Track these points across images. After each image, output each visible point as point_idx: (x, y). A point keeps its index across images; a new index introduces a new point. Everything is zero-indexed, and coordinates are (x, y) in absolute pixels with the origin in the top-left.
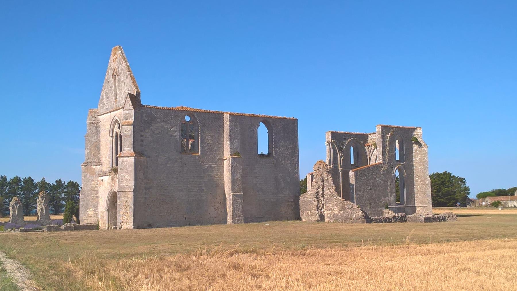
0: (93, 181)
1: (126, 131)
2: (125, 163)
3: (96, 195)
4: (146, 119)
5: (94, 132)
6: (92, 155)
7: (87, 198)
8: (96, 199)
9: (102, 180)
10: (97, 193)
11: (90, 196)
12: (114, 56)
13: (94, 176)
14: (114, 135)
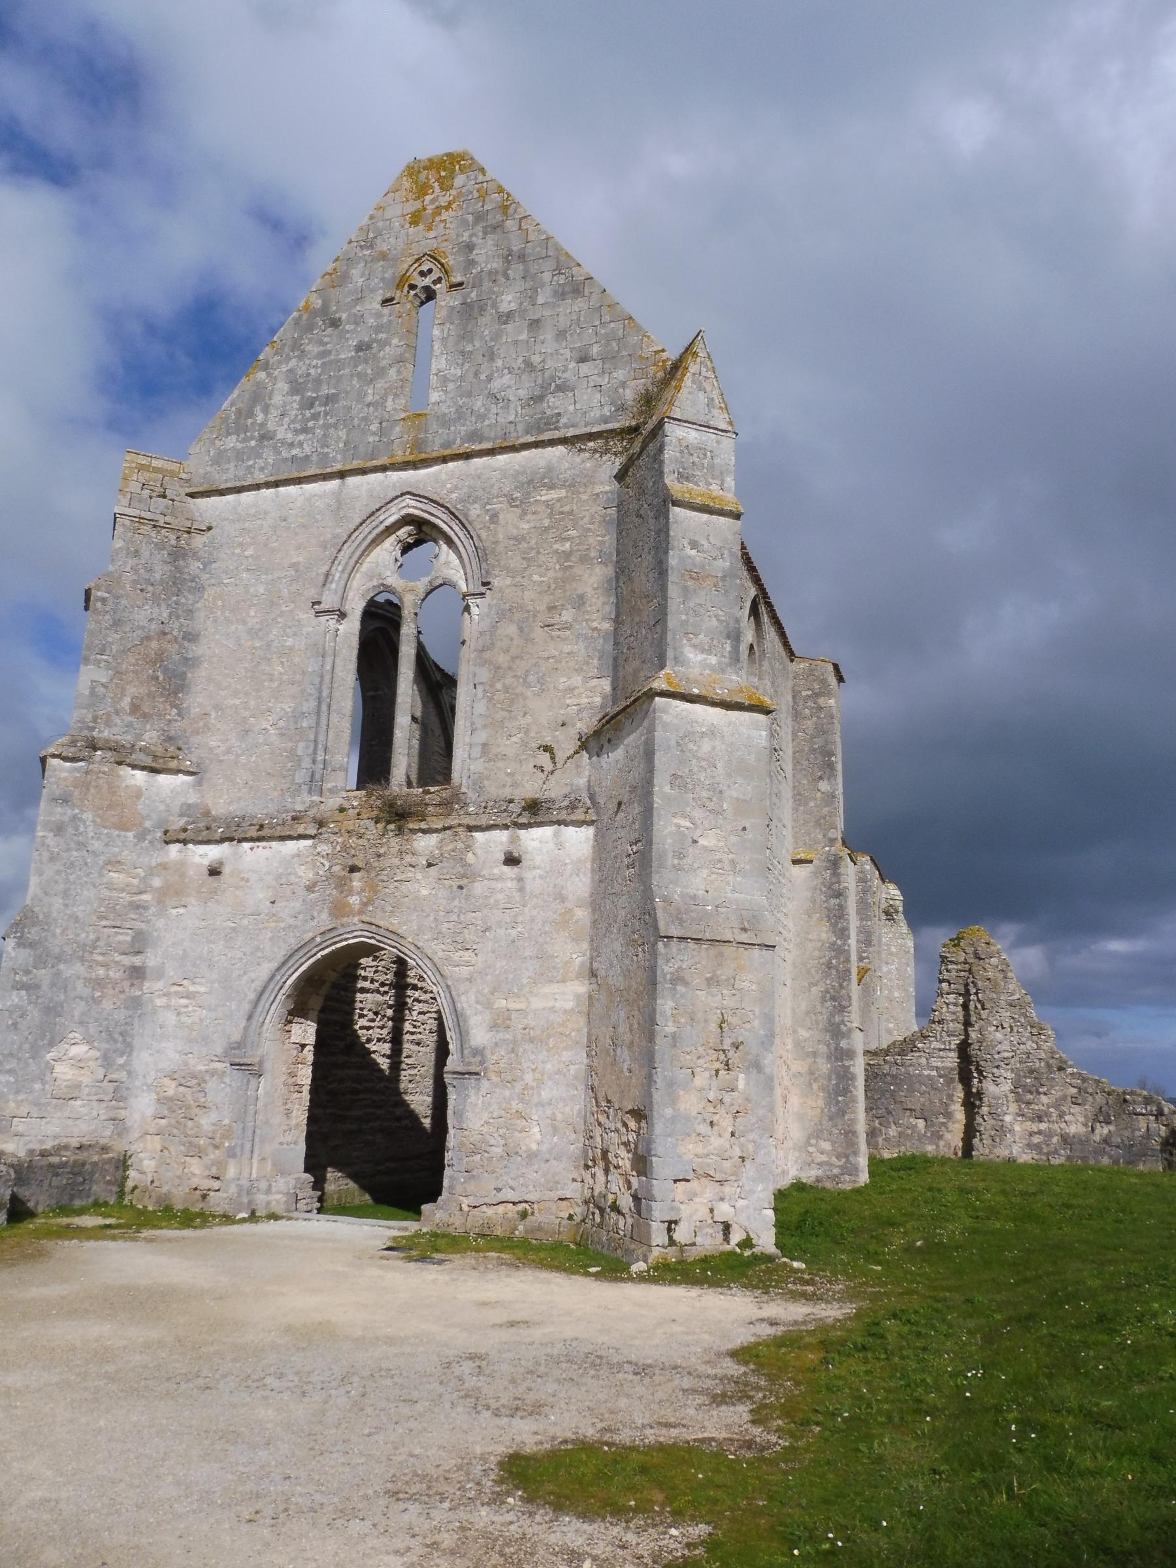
0: (115, 864)
1: (694, 545)
2: (706, 746)
3: (127, 961)
5: (157, 576)
6: (127, 709)
7: (58, 974)
8: (126, 984)
10: (137, 947)
11: (82, 959)
12: (428, 198)
13: (130, 835)
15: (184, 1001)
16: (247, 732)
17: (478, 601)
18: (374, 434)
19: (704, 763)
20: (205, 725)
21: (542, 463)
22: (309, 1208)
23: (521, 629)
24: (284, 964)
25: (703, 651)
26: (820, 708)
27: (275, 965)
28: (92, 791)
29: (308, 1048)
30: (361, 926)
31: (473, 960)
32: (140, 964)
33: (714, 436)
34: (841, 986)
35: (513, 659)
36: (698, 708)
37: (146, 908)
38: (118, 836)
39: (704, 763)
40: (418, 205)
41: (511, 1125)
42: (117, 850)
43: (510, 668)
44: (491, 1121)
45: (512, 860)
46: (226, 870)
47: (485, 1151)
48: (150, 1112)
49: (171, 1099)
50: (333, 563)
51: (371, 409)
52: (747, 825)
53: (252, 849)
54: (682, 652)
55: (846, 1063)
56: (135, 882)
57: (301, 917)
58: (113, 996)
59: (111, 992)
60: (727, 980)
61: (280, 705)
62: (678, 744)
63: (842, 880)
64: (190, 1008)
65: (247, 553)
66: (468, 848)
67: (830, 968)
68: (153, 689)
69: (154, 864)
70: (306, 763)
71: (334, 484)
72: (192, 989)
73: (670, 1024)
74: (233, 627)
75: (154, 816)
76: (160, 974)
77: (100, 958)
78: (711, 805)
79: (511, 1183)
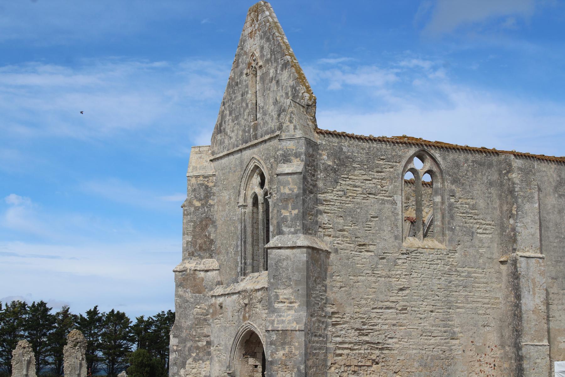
4: (330, 163)
14: (250, 201)
15: (219, 352)
16: (228, 253)
19: (284, 269)
24: (235, 338)
25: (289, 227)
26: (509, 179)
28: (189, 281)
30: (249, 324)
32: (209, 340)
33: (296, 141)
36: (282, 251)
37: (209, 320)
38: (198, 296)
39: (284, 269)
42: (198, 301)
52: (299, 289)
54: (282, 230)
56: (205, 311)
59: (202, 350)
60: (288, 342)
62: (275, 264)
68: (205, 239)
69: (210, 304)
72: (220, 348)
73: (270, 358)
75: (208, 287)
77: (197, 339)
78: (287, 284)
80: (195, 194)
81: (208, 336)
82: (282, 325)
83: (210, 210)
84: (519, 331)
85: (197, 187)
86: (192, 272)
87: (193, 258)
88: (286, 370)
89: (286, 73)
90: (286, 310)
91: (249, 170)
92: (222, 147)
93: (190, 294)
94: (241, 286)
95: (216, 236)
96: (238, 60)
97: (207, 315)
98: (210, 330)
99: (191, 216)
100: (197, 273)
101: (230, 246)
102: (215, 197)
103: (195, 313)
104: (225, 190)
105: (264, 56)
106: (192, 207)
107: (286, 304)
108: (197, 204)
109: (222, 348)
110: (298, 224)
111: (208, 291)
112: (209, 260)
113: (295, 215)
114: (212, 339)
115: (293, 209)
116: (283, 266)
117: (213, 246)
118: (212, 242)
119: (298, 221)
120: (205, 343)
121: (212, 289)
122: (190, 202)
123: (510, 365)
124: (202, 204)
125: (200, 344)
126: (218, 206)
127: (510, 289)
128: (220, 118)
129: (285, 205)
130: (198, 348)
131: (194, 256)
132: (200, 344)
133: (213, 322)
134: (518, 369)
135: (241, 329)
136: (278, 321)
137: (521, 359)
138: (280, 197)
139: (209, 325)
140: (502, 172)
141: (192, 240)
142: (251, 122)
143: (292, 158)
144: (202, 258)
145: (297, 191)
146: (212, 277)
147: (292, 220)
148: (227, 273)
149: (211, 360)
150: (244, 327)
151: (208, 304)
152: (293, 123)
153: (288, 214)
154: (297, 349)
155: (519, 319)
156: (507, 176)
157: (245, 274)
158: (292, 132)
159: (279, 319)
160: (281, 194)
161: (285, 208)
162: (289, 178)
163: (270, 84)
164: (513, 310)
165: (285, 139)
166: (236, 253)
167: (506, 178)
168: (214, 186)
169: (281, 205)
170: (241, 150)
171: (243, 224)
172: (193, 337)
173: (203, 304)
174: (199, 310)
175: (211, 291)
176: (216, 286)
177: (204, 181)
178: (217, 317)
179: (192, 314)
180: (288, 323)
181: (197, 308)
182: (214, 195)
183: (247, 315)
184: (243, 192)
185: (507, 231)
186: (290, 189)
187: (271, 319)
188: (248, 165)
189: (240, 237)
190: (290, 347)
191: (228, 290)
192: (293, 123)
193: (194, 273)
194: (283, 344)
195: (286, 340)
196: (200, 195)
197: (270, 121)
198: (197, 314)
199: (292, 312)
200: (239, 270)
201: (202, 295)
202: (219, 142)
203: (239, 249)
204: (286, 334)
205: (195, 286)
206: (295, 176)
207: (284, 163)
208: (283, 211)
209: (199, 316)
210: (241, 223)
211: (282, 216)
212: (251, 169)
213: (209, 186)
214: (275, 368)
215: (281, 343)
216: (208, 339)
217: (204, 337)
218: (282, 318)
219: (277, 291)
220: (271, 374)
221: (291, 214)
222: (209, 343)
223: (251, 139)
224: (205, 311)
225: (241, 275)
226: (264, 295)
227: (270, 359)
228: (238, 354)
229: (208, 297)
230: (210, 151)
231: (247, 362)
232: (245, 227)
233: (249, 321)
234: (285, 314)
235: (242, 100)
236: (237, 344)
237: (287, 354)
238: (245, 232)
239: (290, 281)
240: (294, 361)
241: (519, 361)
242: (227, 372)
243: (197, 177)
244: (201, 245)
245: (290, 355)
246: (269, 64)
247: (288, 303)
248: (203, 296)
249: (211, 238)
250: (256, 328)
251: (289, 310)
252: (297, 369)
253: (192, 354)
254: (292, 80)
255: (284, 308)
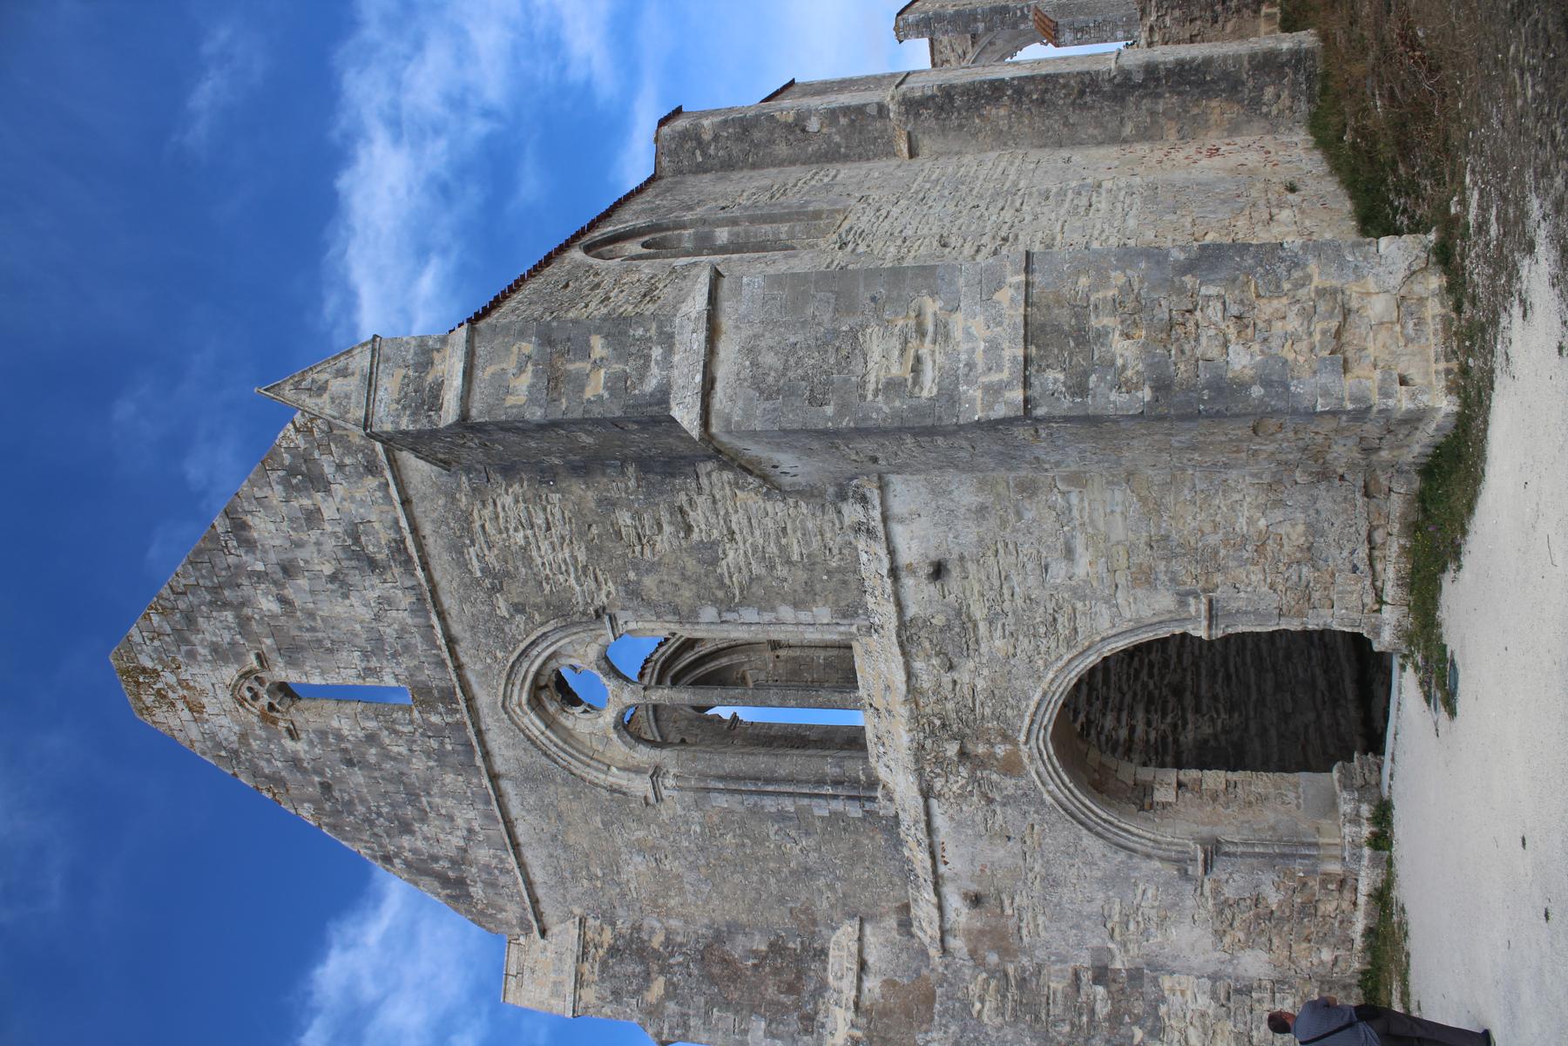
2: (769, 359)
9: (976, 901)
15: (1132, 926)
16: (807, 870)
17: (620, 622)
18: (442, 744)
19: (792, 361)
20: (804, 912)
21: (446, 557)
22: (1375, 768)
23: (648, 571)
24: (1082, 823)
25: (646, 366)
26: (716, 138)
27: (1085, 831)
28: (891, 1035)
29: (1182, 777)
31: (1068, 609)
32: (1090, 973)
34: (1064, 86)
35: (684, 577)
36: (723, 372)
37: (1024, 970)
38: (941, 1004)
39: (792, 361)
40: (180, 705)
41: (1274, 557)
42: (957, 1005)
43: (697, 581)
44: (1269, 580)
45: (938, 571)
46: (974, 888)
47: (1307, 586)
48: (1265, 956)
49: (1249, 934)
50: (596, 785)
51: (415, 747)
53: (946, 863)
54: (651, 395)
55: (1163, 73)
56: (993, 983)
57: (1025, 807)
58: (1129, 1001)
59: (1124, 1004)
60: (1076, 316)
61: (772, 837)
63: (930, 93)
64: (1140, 919)
65: (600, 874)
66: (927, 623)
67: (1043, 102)
68: (767, 969)
69: (971, 963)
70: (838, 806)
71: (506, 785)
72: (1116, 918)
73: (1140, 394)
74: (688, 887)
75: (914, 966)
76: (1101, 953)
77: (1085, 1019)
79: (1345, 554)
80: (628, 991)
81: (1077, 976)
82: (1006, 345)
83: (681, 945)
84: (1082, 82)
85: (607, 984)
86: (863, 1021)
87: (820, 1017)
88: (1191, 326)
89: (257, 521)
90: (950, 349)
91: (548, 738)
92: (502, 880)
93: (934, 1035)
94: (901, 784)
95: (761, 931)
96: (267, 777)
97: (1006, 975)
98: (1058, 967)
99: (691, 1012)
100: (866, 1002)
101: (783, 857)
102: (645, 926)
103: (999, 1020)
104: (618, 873)
105: (233, 644)
106: (664, 1007)
107: (924, 352)
108: (658, 987)
109: (1117, 908)
110: (640, 331)
111: (927, 966)
112: (831, 960)
113: (608, 345)
114: (1085, 960)
115: (585, 352)
116: (779, 365)
117: (791, 945)
118: (776, 948)
119: (631, 332)
120: (1100, 990)
121: (923, 953)
122: (650, 1013)
123: (1171, 119)
124: (661, 972)
125: (1102, 1010)
126: (668, 916)
127: (977, 121)
128: (426, 880)
129: (570, 387)
130: (1115, 1018)
131: (816, 1013)
132: (1102, 1010)
133: (1028, 952)
134: (1180, 84)
135: (1052, 787)
136: (990, 369)
137: (1152, 72)
138: (541, 406)
139: (1039, 969)
140: (698, 164)
141: (764, 1016)
142: (411, 722)
143: (430, 378)
144: (823, 986)
145: (530, 342)
146: (885, 950)
147: (623, 356)
148: (870, 880)
149: (1158, 968)
150: (1042, 769)
151: (969, 967)
152: (327, 381)
153: (602, 372)
154: (1102, 281)
155: (1050, 87)
156: (709, 144)
157: (873, 783)
158: (353, 385)
159: (980, 367)
160: (532, 400)
161: (580, 382)
162: (483, 375)
163: (299, 613)
164: (1029, 109)
165: (368, 405)
166: (802, 822)
167: (712, 151)
168: (613, 924)
169: (568, 399)
170: (494, 777)
171: (713, 784)
172: (1078, 1035)
173: (971, 987)
174: (987, 1005)
175: (928, 957)
176: (912, 936)
177: (594, 959)
178: (1012, 923)
179: (999, 1029)
180: (999, 324)
181: (980, 1012)
182: (639, 929)
183: (1001, 750)
184: (617, 778)
185: (837, 139)
186: (521, 370)
187: (979, 402)
188: (529, 739)
189: (752, 800)
190: (1096, 307)
191: (921, 859)
192: (327, 381)
193: (867, 1013)
194: (1082, 337)
195: (1066, 328)
196: (635, 976)
197: (394, 613)
198: (1000, 1011)
199: (958, 322)
200: (854, 811)
201: (939, 991)
202: (490, 891)
203: (789, 805)
204: (1042, 327)
205: (908, 1014)
206: (481, 351)
207: (441, 408)
208: (589, 394)
209: (1010, 1005)
210: (708, 790)
211: (606, 395)
212: (543, 728)
213: (612, 942)
214: (1183, 370)
215: (1077, 345)
216: (1086, 977)
217: (1078, 990)
218: (979, 358)
219: (871, 387)
220: (1208, 386)
221: (602, 359)
222: (1102, 975)
223: (457, 723)
224: (993, 983)
225: (873, 799)
226: (927, 644)
227: (1146, 394)
228: (1139, 829)
229: (946, 967)
230: (522, 940)
231: (1165, 805)
232: (721, 778)
233: (1022, 738)
234: (964, 347)
235: (364, 764)
236: (1101, 818)
237: (1122, 322)
238: (738, 778)
239: (836, 333)
240: (1153, 288)
241: (1158, 80)
242: (1200, 869)
243: (579, 982)
244: (784, 987)
245: (1130, 305)
246: (249, 619)
247: (922, 342)
248: (941, 986)
249: (763, 948)
250: (1045, 694)
251: (947, 337)
252: (1184, 274)
253: (1136, 1041)
254: (267, 491)
255: (940, 358)
